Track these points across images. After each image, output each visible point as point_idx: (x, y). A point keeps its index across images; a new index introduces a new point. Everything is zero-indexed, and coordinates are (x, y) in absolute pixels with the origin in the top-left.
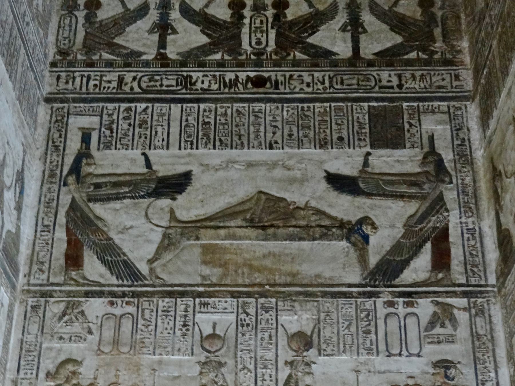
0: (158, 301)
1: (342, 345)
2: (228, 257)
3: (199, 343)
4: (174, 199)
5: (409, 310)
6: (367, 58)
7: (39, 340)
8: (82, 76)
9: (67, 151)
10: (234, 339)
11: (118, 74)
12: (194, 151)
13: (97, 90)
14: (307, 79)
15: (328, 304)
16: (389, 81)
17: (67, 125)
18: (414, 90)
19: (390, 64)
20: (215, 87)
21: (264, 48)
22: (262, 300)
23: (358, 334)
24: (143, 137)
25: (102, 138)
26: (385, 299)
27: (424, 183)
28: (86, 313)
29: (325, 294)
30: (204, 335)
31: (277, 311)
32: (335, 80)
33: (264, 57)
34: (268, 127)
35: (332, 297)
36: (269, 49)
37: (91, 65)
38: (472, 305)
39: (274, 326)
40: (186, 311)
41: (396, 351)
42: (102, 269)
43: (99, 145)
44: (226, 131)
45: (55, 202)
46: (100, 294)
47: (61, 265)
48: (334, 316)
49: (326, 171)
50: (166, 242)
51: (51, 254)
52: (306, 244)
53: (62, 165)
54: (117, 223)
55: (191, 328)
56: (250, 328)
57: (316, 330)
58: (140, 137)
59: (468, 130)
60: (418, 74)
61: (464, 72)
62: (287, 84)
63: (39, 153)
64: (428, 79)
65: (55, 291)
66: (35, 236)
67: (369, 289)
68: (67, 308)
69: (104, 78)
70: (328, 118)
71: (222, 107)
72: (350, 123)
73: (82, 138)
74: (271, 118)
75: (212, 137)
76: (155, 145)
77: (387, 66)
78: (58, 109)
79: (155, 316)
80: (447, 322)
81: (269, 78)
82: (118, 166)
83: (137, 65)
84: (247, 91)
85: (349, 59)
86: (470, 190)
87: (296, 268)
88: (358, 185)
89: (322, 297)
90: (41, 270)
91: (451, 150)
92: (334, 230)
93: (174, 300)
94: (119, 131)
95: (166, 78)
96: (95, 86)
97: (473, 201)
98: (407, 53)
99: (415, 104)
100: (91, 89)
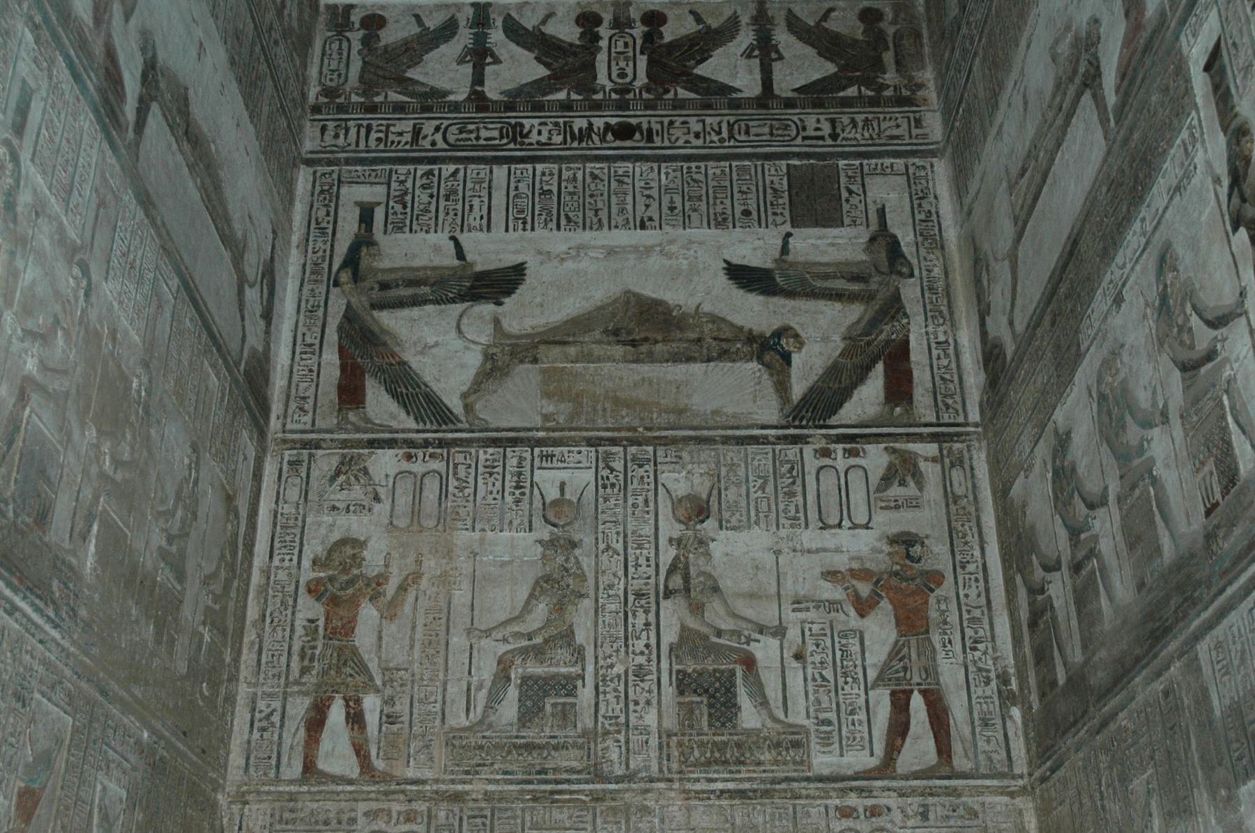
0: (477, 452)
1: (753, 513)
2: (580, 386)
3: (541, 513)
4: (499, 304)
5: (853, 461)
6: (784, 95)
7: (301, 512)
8: (359, 126)
9: (338, 235)
10: (593, 506)
11: (412, 122)
12: (528, 233)
13: (382, 147)
14: (697, 127)
15: (732, 453)
16: (817, 129)
17: (338, 198)
18: (854, 143)
19: (818, 104)
20: (558, 139)
21: (631, 83)
22: (633, 450)
23: (776, 498)
24: (452, 213)
25: (390, 217)
26: (817, 446)
27: (870, 276)
28: (370, 471)
29: (726, 440)
30: (548, 501)
31: (655, 465)
32: (736, 127)
33: (631, 96)
34: (638, 196)
35: (737, 444)
36: (638, 84)
37: (373, 109)
38: (945, 452)
39: (652, 486)
40: (520, 465)
41: (833, 520)
42: (392, 406)
43: (386, 225)
44: (576, 204)
45: (322, 309)
46: (391, 444)
47: (331, 401)
48: (741, 472)
49: (725, 261)
50: (489, 366)
51: (317, 386)
52: (697, 368)
53: (331, 256)
54: (415, 338)
55: (527, 491)
56: (616, 490)
57: (715, 492)
58: (447, 214)
59: (936, 197)
60: (860, 118)
61: (929, 115)
62: (666, 135)
63: (295, 239)
64: (875, 124)
65: (324, 440)
66: (293, 359)
67: (792, 431)
68: (342, 463)
69: (392, 129)
70: (728, 184)
71: (569, 169)
72: (761, 189)
73: (361, 215)
74: (642, 184)
75: (555, 212)
76: (469, 225)
77: (814, 106)
78: (324, 174)
79: (473, 474)
80: (909, 478)
81: (639, 126)
82: (415, 256)
83: (442, 107)
84: (605, 145)
85: (757, 98)
86: (940, 285)
87: (683, 401)
88: (774, 280)
89: (723, 443)
90: (301, 409)
91: (910, 228)
92: (739, 346)
93: (501, 450)
94: (416, 205)
95: (486, 128)
96: (379, 140)
97: (945, 302)
98: (844, 88)
99: (857, 162)
100: (372, 143)
